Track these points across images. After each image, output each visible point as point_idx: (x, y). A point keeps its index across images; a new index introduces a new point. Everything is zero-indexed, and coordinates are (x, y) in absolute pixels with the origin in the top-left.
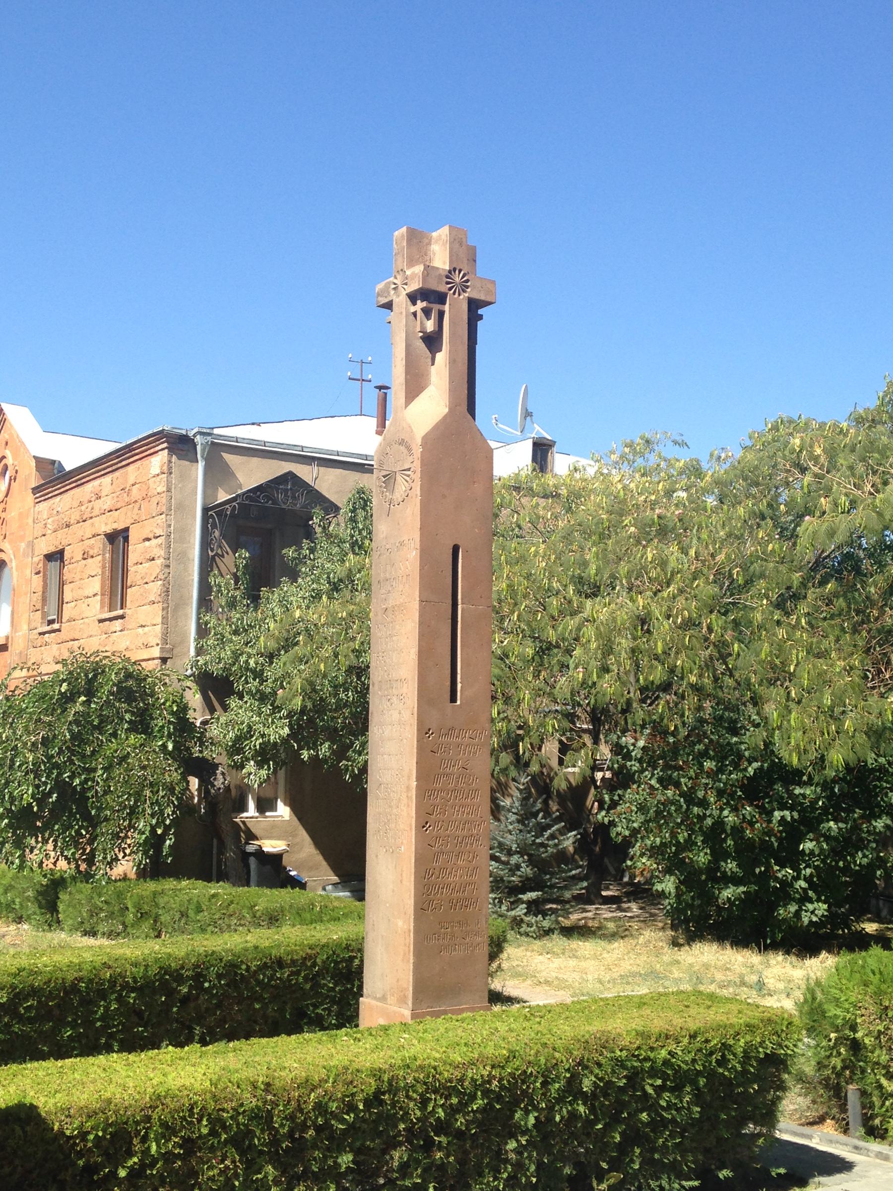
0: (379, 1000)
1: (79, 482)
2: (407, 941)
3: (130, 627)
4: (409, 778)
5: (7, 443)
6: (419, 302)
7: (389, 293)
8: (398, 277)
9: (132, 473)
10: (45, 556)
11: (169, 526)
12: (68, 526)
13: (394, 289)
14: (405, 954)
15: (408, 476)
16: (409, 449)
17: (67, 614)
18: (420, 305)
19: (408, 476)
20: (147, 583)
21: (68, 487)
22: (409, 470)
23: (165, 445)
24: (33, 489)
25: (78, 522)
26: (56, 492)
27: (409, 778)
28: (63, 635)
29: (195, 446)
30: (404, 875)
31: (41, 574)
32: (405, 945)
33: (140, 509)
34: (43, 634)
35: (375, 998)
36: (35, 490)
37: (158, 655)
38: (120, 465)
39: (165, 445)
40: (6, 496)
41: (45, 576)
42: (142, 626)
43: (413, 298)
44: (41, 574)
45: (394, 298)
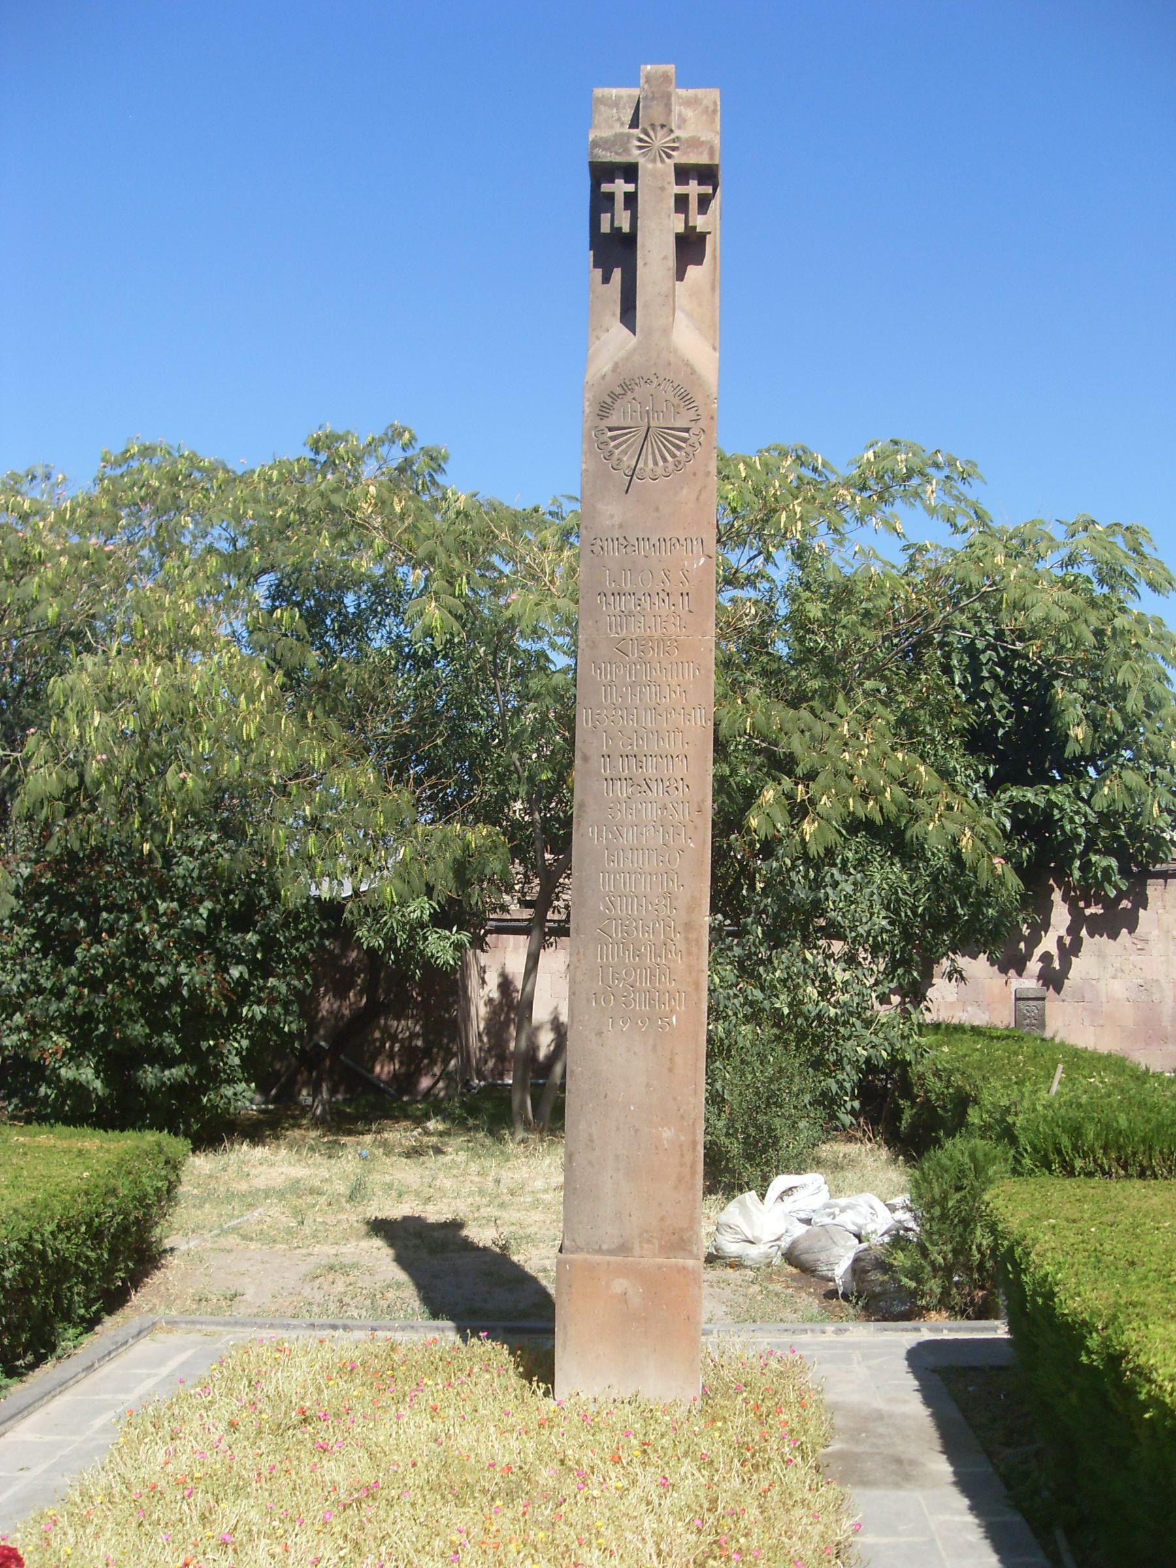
0: (611, 1252)
2: (688, 1158)
4: (690, 909)
6: (693, 183)
7: (627, 151)
8: (652, 133)
13: (640, 148)
14: (680, 1179)
15: (684, 440)
16: (686, 399)
18: (693, 189)
19: (684, 440)
22: (687, 430)
27: (690, 909)
30: (679, 1060)
32: (682, 1165)
35: (600, 1251)
43: (683, 173)
45: (641, 161)
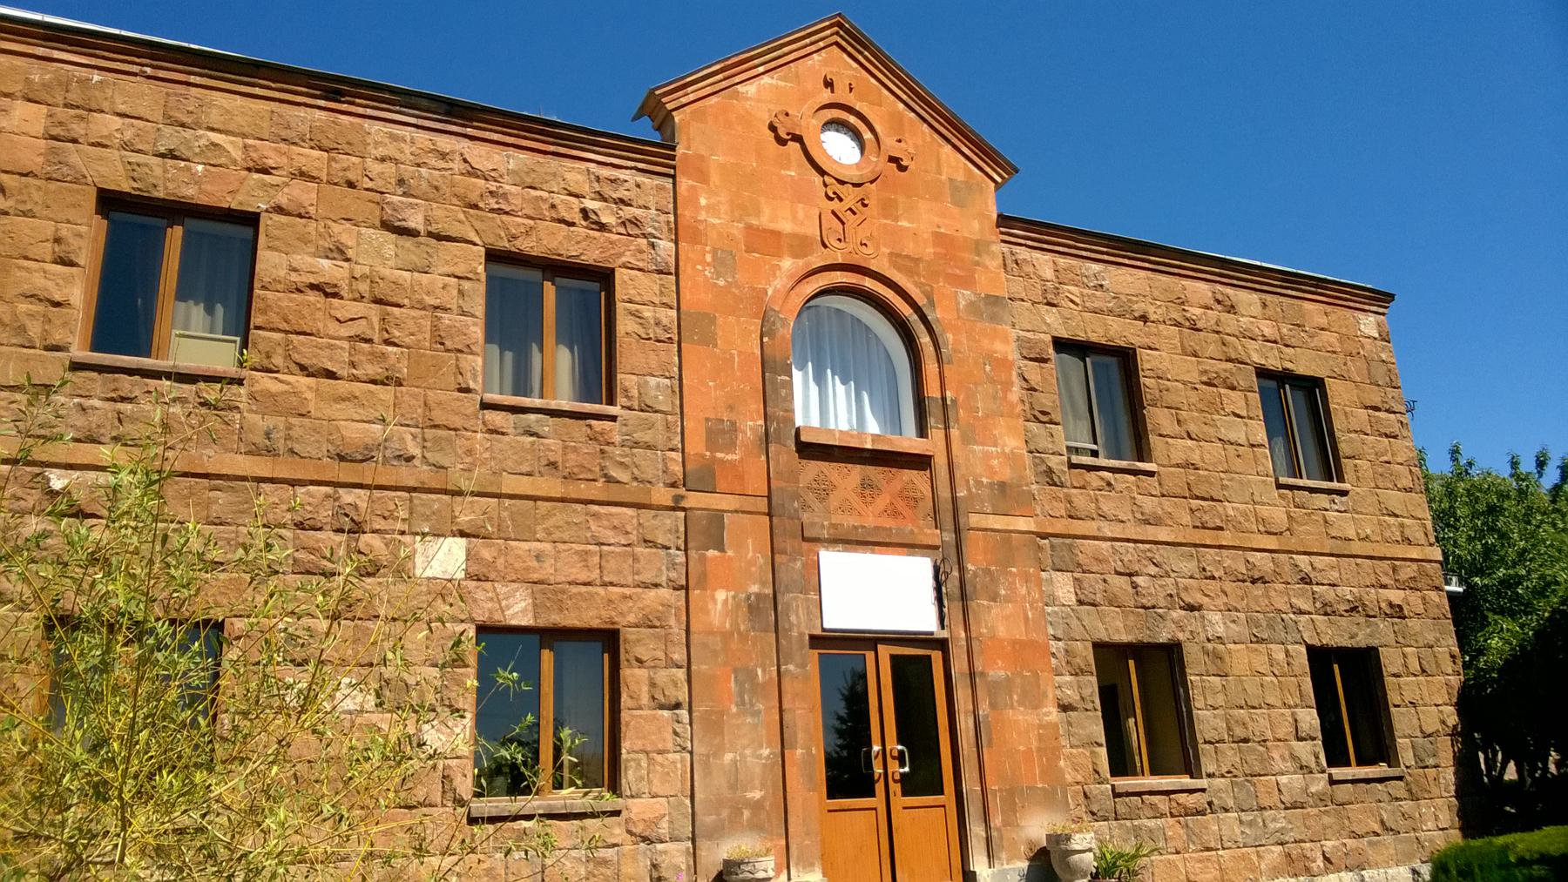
3: (1364, 511)
12: (1144, 318)
20: (1389, 463)
26: (1084, 253)
33: (1345, 364)
38: (1279, 290)
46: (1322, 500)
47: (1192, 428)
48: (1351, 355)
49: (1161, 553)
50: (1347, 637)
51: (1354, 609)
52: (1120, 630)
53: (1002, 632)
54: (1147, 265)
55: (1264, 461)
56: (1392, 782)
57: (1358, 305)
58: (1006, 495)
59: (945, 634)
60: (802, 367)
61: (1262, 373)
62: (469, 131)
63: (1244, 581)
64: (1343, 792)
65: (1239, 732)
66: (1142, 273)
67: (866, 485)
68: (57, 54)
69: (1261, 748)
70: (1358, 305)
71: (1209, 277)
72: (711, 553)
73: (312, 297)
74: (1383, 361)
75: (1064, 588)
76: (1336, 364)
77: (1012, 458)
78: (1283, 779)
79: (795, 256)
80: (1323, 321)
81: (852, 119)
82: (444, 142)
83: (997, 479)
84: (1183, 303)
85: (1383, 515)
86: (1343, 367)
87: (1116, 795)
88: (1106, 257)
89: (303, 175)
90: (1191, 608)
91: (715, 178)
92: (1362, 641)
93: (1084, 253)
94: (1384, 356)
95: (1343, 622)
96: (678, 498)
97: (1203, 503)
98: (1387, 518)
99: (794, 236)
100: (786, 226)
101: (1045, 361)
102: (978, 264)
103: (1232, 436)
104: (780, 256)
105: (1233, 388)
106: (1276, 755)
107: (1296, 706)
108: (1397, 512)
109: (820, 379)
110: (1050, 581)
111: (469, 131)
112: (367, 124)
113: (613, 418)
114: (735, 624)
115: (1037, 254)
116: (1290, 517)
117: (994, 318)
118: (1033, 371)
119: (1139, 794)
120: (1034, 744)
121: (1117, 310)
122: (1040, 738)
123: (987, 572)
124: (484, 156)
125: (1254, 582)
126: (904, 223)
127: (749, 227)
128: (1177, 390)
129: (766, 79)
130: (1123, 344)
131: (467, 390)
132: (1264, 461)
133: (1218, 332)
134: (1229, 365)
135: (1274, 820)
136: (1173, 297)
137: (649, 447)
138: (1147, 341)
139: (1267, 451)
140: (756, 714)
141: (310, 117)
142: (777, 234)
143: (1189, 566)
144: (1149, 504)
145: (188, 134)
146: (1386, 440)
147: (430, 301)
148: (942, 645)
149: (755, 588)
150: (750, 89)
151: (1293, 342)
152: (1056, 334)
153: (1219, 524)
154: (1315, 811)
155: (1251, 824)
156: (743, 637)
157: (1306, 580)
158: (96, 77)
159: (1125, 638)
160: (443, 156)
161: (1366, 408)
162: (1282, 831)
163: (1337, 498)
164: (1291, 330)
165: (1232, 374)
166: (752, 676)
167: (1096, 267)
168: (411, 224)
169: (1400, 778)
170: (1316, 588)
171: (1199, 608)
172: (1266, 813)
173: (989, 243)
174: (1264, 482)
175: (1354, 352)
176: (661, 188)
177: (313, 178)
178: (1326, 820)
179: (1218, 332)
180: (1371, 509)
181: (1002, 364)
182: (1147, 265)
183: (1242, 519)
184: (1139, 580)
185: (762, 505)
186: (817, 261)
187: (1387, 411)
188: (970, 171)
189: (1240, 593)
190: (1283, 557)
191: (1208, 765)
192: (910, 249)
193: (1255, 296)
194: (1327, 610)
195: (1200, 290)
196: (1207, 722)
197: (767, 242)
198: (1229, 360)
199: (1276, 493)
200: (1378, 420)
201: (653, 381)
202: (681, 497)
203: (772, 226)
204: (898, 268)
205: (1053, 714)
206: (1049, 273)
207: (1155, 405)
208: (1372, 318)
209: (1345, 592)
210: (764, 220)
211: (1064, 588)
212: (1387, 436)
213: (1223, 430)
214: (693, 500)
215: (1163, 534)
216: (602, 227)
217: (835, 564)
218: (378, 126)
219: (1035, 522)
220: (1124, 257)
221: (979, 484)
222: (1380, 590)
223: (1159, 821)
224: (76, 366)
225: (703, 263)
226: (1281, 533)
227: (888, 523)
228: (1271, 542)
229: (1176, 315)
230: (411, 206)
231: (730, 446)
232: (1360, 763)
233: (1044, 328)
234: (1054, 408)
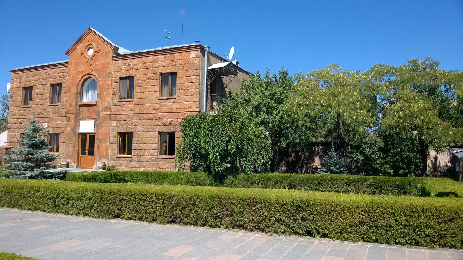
1: (143, 56)
5: (92, 41)
9: (178, 56)
10: (119, 78)
11: (200, 73)
12: (136, 69)
17: (136, 96)
20: (189, 89)
21: (135, 57)
23: (200, 49)
24: (112, 57)
25: (143, 68)
26: (127, 58)
28: (133, 103)
29: (205, 51)
31: (118, 83)
33: (184, 67)
34: (122, 102)
36: (113, 57)
37: (198, 111)
38: (169, 53)
39: (200, 49)
40: (93, 57)
41: (119, 84)
42: (187, 102)
44: (118, 83)
46: (169, 101)
47: (142, 90)
48: (186, 64)
49: (131, 116)
50: (168, 129)
51: (170, 124)
52: (123, 130)
53: (103, 132)
54: (140, 57)
55: (157, 94)
56: (171, 159)
57: (191, 50)
58: (107, 109)
59: (95, 132)
60: (91, 90)
61: (161, 74)
62: (49, 68)
63: (147, 120)
64: (159, 160)
65: (140, 148)
66: (139, 59)
67: (88, 110)
68: (19, 72)
69: (144, 151)
70: (191, 50)
71: (153, 55)
72: (68, 122)
73: (36, 95)
74: (195, 63)
75: (114, 123)
76: (181, 68)
77: (109, 102)
78: (147, 157)
79: (81, 75)
80: (179, 58)
81: (92, 46)
82: (46, 71)
83: (105, 106)
84: (146, 63)
85: (184, 102)
86: (182, 68)
87: (117, 157)
88: (132, 58)
89: (35, 80)
90: (135, 126)
91: (73, 65)
92: (172, 130)
93: (127, 58)
94: (195, 62)
95: (168, 127)
96: (66, 115)
97: (141, 105)
98: (186, 103)
99: (82, 71)
100: (81, 70)
101: (117, 83)
102: (108, 67)
103: (150, 90)
104: (79, 75)
105: (153, 80)
106: (146, 152)
107: (153, 143)
108: (188, 101)
109: (94, 91)
110: (112, 123)
111: (49, 68)
112: (40, 71)
113: (60, 105)
114: (70, 132)
115: (119, 62)
116: (160, 106)
117: (109, 77)
118: (114, 85)
119: (120, 157)
120: (105, 149)
121: (131, 69)
122: (106, 148)
123: (102, 122)
124: (49, 71)
125: (149, 120)
126: (97, 63)
127: (76, 71)
128: (141, 83)
129: (81, 44)
130: (132, 76)
131: (47, 104)
132: (157, 94)
133: (152, 68)
134: (154, 75)
135: (144, 164)
136: (143, 62)
137: (64, 108)
138: (136, 74)
139: (158, 92)
140: (71, 144)
141: (37, 72)
142: (79, 71)
143: (136, 118)
144: (130, 107)
145: (27, 78)
146: (190, 84)
147: (45, 93)
148: (95, 133)
149: (72, 127)
150: (78, 47)
151: (170, 65)
152: (120, 77)
153: (143, 109)
154: (153, 163)
155: (139, 164)
156: (71, 133)
157: (160, 119)
158: (22, 74)
159: (123, 132)
160: (46, 73)
161: (187, 77)
162: (145, 166)
163: (172, 100)
164: (170, 62)
165: (153, 76)
166: (71, 138)
167: (129, 60)
168: (43, 84)
169: (174, 158)
170: (162, 120)
171: (137, 126)
172: (142, 162)
173: (110, 62)
174: (156, 99)
175: (186, 63)
176: (67, 69)
177: (36, 80)
178: (155, 165)
179: (152, 68)
180: (181, 101)
181: (109, 85)
182: (140, 57)
183: (149, 107)
184: (127, 121)
185: (74, 115)
186: (83, 75)
187: (193, 76)
188: (109, 49)
189: (146, 122)
190: (156, 114)
191: (133, 154)
192: (98, 68)
193: (164, 56)
194: (164, 124)
195: (150, 59)
196: (134, 145)
197: (78, 73)
198: (154, 73)
199: (158, 101)
200: (189, 79)
201: (64, 99)
202: (66, 115)
203: (79, 70)
204: (95, 72)
205: (108, 144)
206: (120, 65)
207: (136, 87)
208: (195, 52)
209: (169, 120)
210: (78, 70)
211: (114, 123)
212: (191, 83)
213: (149, 89)
214: (67, 115)
215: (132, 112)
216: (61, 77)
217: (82, 122)
218: (42, 71)
219: (111, 113)
220: (135, 57)
221: (103, 107)
222: (179, 119)
223: (122, 162)
224: (21, 108)
225: (70, 79)
226: (157, 109)
227: (90, 116)
228: (154, 112)
229: (143, 67)
230: (43, 81)
231: (71, 107)
232: (169, 155)
233: (118, 76)
234: (116, 92)
